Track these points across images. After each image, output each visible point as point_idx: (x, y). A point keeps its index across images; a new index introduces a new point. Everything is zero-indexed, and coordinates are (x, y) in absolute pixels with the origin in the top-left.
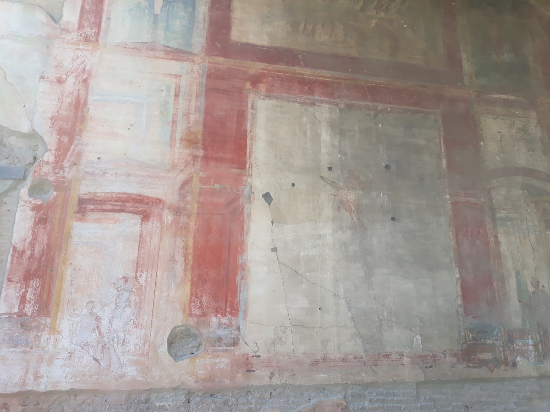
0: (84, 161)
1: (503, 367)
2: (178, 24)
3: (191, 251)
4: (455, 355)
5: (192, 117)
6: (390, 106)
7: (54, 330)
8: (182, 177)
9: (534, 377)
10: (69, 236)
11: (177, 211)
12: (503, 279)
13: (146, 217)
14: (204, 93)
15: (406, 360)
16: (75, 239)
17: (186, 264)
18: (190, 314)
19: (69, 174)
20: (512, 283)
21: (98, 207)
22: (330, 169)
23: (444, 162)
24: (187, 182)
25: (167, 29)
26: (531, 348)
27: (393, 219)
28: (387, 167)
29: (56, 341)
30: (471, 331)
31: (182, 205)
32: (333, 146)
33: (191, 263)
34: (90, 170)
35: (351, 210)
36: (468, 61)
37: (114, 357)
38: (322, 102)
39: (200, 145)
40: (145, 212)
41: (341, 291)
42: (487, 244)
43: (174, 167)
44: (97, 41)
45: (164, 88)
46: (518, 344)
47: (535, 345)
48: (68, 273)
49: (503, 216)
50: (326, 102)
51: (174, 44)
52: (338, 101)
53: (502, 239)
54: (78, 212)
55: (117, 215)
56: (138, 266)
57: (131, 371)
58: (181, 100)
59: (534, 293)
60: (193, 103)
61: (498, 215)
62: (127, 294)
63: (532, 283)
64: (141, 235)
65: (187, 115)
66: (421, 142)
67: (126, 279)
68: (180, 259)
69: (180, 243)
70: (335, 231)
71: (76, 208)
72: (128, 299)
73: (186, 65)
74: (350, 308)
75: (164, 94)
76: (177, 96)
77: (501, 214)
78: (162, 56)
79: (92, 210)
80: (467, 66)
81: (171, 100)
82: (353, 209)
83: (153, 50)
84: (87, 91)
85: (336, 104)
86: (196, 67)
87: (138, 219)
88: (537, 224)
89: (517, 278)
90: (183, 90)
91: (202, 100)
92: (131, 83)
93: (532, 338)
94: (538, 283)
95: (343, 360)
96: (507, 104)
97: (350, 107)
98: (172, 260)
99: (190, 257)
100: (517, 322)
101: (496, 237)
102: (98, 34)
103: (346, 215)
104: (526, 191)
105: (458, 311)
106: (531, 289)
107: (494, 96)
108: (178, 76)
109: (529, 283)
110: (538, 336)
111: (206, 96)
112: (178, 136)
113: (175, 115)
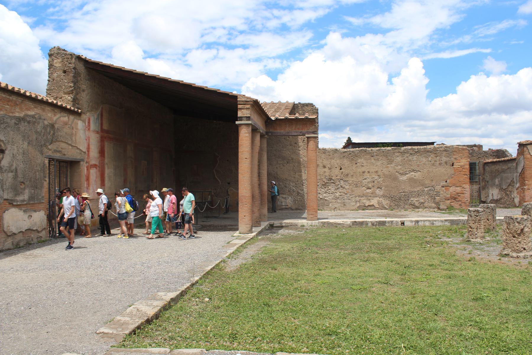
11: (99, 167)
13: (96, 168)
19: (89, 160)
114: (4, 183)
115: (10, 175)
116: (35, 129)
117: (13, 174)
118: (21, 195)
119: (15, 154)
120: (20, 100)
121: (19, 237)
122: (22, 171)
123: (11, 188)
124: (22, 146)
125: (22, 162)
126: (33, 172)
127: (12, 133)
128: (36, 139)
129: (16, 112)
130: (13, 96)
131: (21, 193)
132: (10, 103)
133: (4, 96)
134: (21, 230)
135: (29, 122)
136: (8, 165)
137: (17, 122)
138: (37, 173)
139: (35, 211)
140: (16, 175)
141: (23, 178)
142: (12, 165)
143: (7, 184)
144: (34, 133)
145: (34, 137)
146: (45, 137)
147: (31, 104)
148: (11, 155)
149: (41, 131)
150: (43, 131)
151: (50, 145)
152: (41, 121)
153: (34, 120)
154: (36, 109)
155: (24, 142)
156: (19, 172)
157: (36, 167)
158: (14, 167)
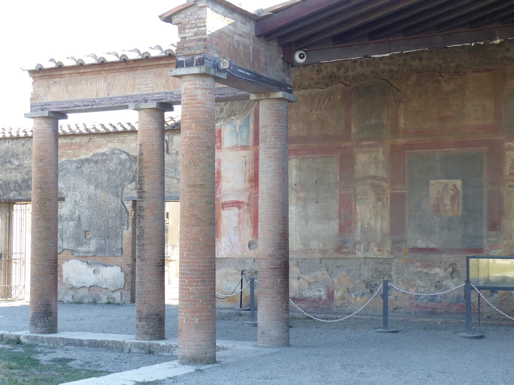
0: (222, 191)
1: (351, 254)
2: (244, 135)
3: (252, 218)
4: (334, 250)
5: (251, 171)
6: (319, 155)
7: (220, 242)
8: (249, 193)
9: (362, 258)
10: (221, 215)
11: (248, 205)
12: (355, 223)
13: (240, 208)
14: (254, 161)
15: (317, 251)
16: (222, 216)
17: (251, 222)
18: (253, 237)
20: (359, 224)
21: (227, 206)
22: (295, 185)
23: (338, 177)
24: (250, 195)
25: (241, 138)
26: (362, 248)
27: (316, 202)
28: (316, 182)
29: (221, 245)
30: (341, 242)
31: (249, 203)
32: (297, 175)
33: (253, 221)
34: (224, 194)
35: (302, 200)
36: (354, 127)
37: (235, 249)
38: (293, 158)
39: (253, 181)
40: (239, 206)
41: (297, 229)
42: (351, 209)
43: (246, 190)
44: (221, 148)
45: (242, 162)
46: (358, 246)
47: (364, 247)
48: (222, 226)
49: (359, 197)
50: (295, 158)
51: (243, 144)
52: (299, 156)
53: (358, 207)
54: (222, 208)
55: (232, 208)
56: (239, 223)
57: (239, 253)
58: (247, 165)
59: (367, 228)
60: (251, 166)
61: (357, 198)
62: (237, 231)
63: (367, 224)
64: (239, 214)
65: (249, 171)
66: (330, 170)
67: (236, 227)
68: (249, 220)
69: (249, 216)
70: (296, 208)
71: (221, 206)
72: (237, 233)
73: (247, 151)
74: (300, 235)
75: (242, 164)
76: (245, 164)
77: (359, 197)
78: (240, 149)
79: (226, 207)
80: (353, 130)
81: (244, 166)
82: (303, 200)
83: (237, 147)
84: (220, 167)
85: (298, 158)
86: (251, 152)
87: (238, 208)
88: (374, 200)
89: (361, 222)
90: (247, 161)
91: (253, 164)
92: (232, 162)
93: (363, 244)
94: (370, 224)
95: (297, 251)
96: (369, 146)
97: (303, 158)
98: (248, 221)
99: (252, 220)
100: (358, 238)
101: (355, 206)
102: (221, 145)
103: (300, 202)
104: (371, 186)
105: (337, 235)
106: (366, 226)
107: (364, 143)
108: (245, 156)
109: (366, 223)
110: (366, 244)
111: (254, 163)
112: (247, 179)
113: (245, 171)
114: (64, 232)
115: (72, 223)
116: (106, 168)
117: (76, 222)
118: (85, 245)
119: (77, 201)
120: (86, 139)
121: (83, 292)
122: (88, 219)
123: (73, 238)
124: (87, 191)
125: (88, 208)
126: (104, 219)
127: (73, 178)
128: (108, 180)
129: (81, 154)
130: (76, 139)
131: (85, 243)
132: (72, 148)
133: (65, 141)
134: (84, 285)
135: (96, 162)
136: (69, 213)
137: (80, 166)
138: (110, 220)
139: (105, 265)
140: (79, 223)
141: (89, 226)
142: (74, 213)
143: (68, 234)
144: (104, 173)
145: (105, 178)
146: (122, 175)
147: (103, 139)
148: (73, 202)
149: (116, 169)
150: (119, 168)
151: (130, 184)
152: (114, 157)
153: (105, 157)
154: (110, 144)
155: (90, 186)
156: (83, 219)
157: (109, 213)
158: (76, 215)
